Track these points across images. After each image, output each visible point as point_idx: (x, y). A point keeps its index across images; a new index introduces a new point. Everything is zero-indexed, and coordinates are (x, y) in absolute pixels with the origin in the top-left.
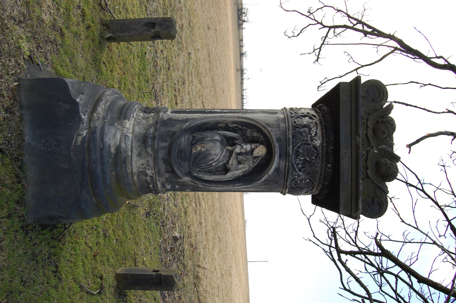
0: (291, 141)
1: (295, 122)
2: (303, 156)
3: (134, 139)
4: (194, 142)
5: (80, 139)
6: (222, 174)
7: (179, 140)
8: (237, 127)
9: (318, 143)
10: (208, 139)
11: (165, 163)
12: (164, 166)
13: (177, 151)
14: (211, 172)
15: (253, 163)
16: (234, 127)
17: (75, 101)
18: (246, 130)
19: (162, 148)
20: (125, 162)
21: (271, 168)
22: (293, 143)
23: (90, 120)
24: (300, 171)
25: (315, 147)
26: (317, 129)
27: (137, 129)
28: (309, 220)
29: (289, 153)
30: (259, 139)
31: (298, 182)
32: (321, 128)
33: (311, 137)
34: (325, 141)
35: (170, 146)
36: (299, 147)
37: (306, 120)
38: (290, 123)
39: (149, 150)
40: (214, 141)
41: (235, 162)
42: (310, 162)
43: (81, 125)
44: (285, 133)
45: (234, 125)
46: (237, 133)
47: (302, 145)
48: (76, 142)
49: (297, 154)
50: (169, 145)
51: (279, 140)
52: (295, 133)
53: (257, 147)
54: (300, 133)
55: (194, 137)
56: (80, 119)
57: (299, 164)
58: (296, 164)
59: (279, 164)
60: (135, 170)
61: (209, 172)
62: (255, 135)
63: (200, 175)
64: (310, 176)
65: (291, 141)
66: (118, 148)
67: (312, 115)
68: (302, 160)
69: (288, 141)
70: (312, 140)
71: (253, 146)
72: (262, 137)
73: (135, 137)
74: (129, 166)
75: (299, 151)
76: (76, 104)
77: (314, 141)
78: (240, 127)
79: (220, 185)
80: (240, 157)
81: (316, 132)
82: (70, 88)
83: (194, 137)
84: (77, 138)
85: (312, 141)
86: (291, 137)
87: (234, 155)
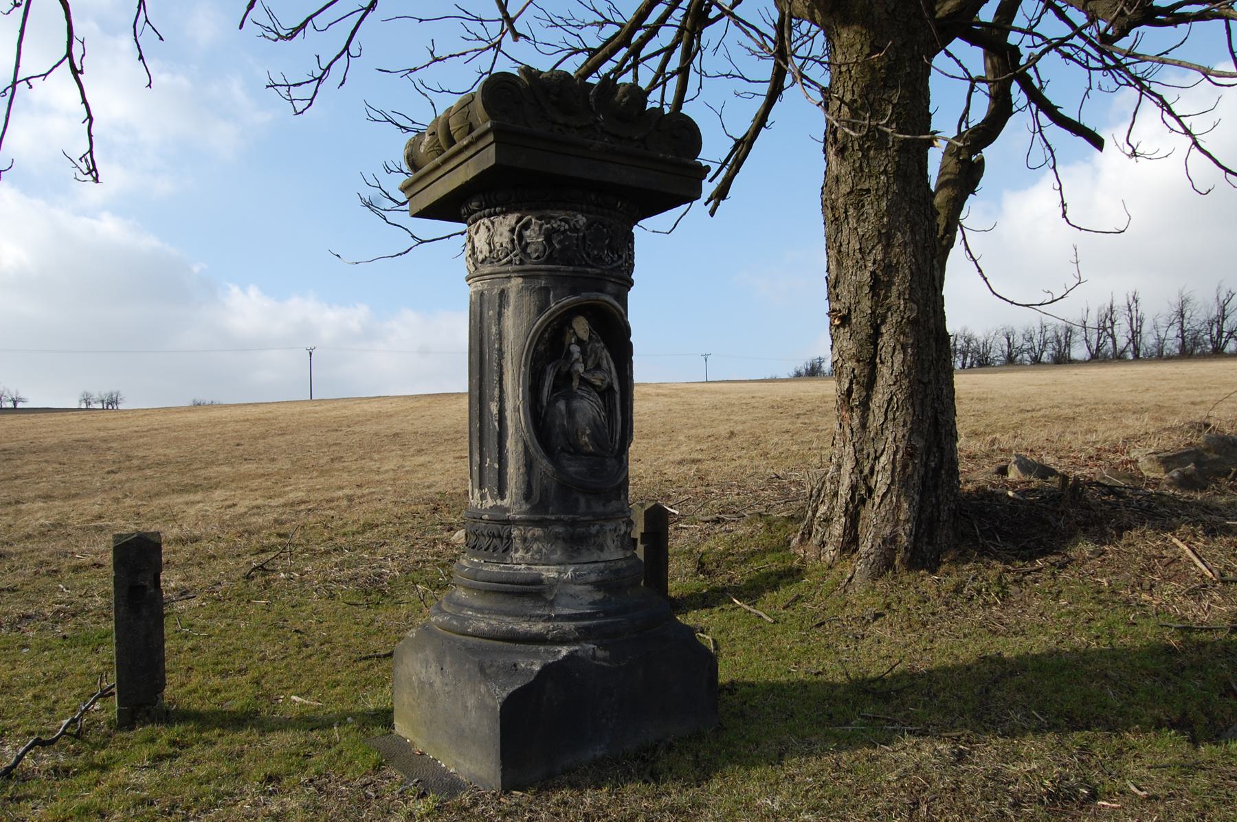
0: (579, 269)
1: (538, 257)
3: (575, 561)
5: (600, 653)
9: (582, 220)
15: (598, 342)
17: (540, 672)
20: (617, 571)
22: (580, 265)
23: (562, 640)
24: (620, 257)
25: (589, 226)
26: (552, 218)
27: (557, 556)
28: (423, 242)
33: (570, 230)
36: (588, 255)
37: (534, 236)
38: (543, 266)
39: (594, 530)
40: (571, 413)
41: (599, 375)
43: (580, 654)
48: (604, 660)
49: (599, 260)
51: (574, 292)
53: (575, 333)
55: (563, 450)
56: (571, 657)
65: (579, 269)
66: (598, 586)
67: (517, 223)
70: (575, 229)
73: (573, 557)
74: (619, 564)
76: (546, 668)
81: (561, 220)
82: (517, 687)
84: (600, 659)
86: (571, 268)
87: (587, 376)
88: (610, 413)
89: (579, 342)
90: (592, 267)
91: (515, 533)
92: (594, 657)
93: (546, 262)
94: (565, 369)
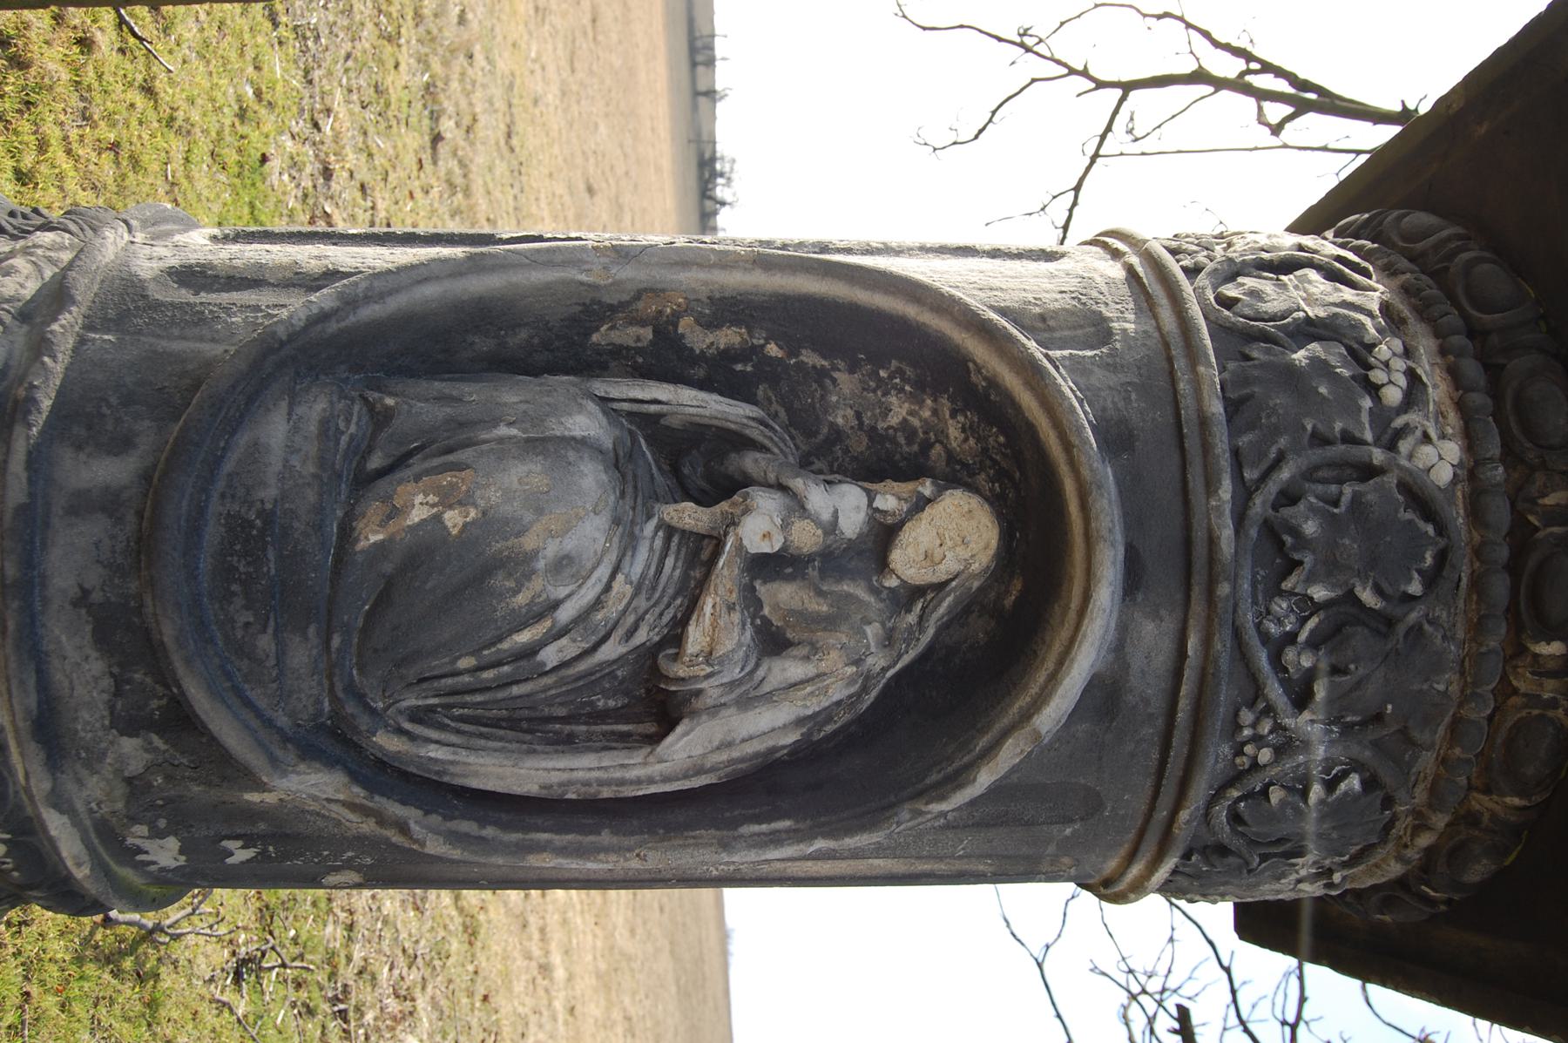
1: (1229, 303)
2: (1330, 568)
4: (375, 462)
6: (624, 737)
7: (243, 439)
8: (749, 352)
9: (1440, 460)
10: (503, 430)
11: (102, 638)
12: (96, 666)
13: (213, 533)
14: (530, 727)
15: (888, 640)
16: (727, 356)
18: (821, 375)
19: (82, 504)
21: (1054, 679)
25: (1416, 495)
28: (1040, 965)
29: (1212, 541)
30: (926, 446)
31: (1276, 795)
32: (1443, 352)
33: (1382, 416)
34: (1495, 450)
35: (153, 483)
36: (1289, 497)
38: (1195, 311)
41: (735, 638)
42: (1384, 623)
45: (729, 337)
46: (750, 399)
47: (1310, 475)
49: (1278, 551)
50: (146, 477)
51: (1116, 437)
52: (1244, 380)
53: (920, 504)
55: (380, 418)
57: (1291, 638)
58: (1265, 638)
59: (1119, 647)
61: (512, 724)
62: (894, 420)
63: (435, 752)
64: (1376, 745)
68: (1317, 607)
69: (1192, 444)
71: (888, 502)
72: (954, 432)
75: (1296, 532)
77: (1404, 446)
78: (773, 350)
79: (606, 837)
80: (783, 596)
81: (1411, 375)
85: (1392, 447)
86: (1216, 408)
87: (727, 574)
90: (1240, 520)
93: (1220, 330)
94: (751, 462)
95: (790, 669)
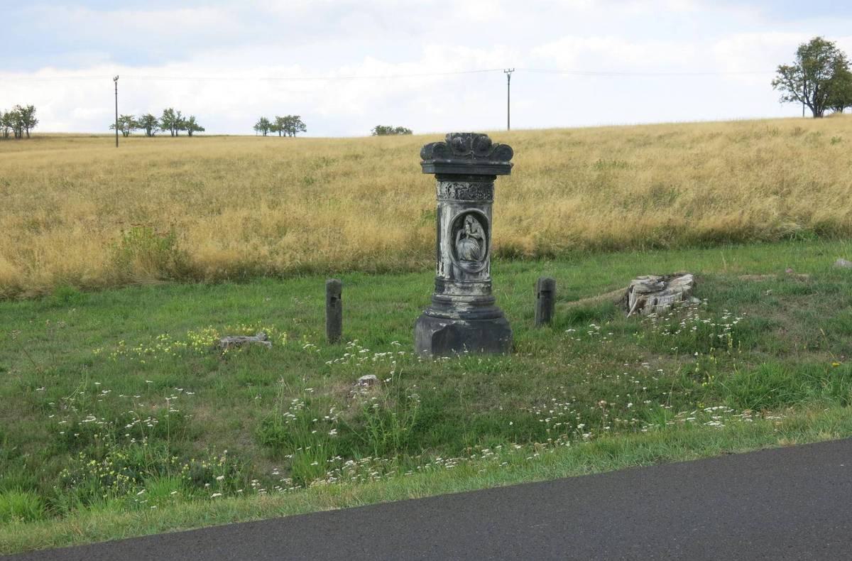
5: (467, 324)
9: (467, 185)
23: (455, 319)
25: (470, 187)
35: (468, 273)
37: (452, 190)
39: (470, 285)
41: (476, 234)
44: (461, 204)
49: (474, 197)
51: (465, 208)
54: (461, 195)
60: (481, 294)
80: (473, 231)
83: (461, 259)
88: (481, 249)
89: (469, 223)
91: (446, 285)
92: (464, 325)
94: (463, 232)
95: (478, 231)
